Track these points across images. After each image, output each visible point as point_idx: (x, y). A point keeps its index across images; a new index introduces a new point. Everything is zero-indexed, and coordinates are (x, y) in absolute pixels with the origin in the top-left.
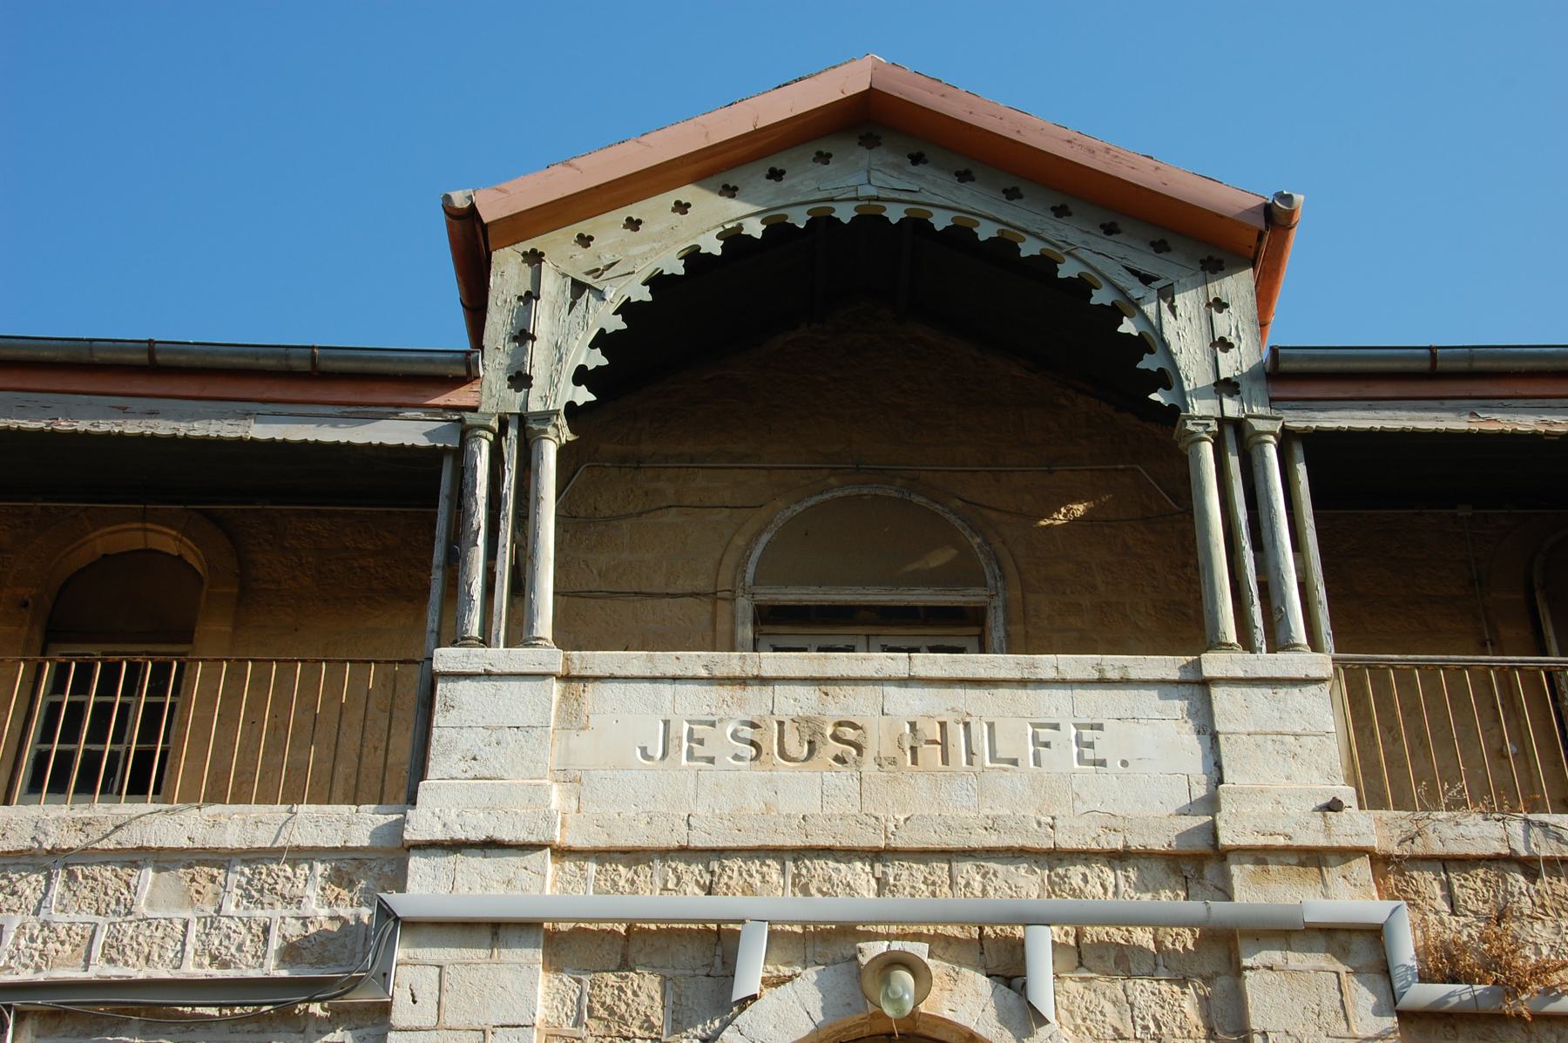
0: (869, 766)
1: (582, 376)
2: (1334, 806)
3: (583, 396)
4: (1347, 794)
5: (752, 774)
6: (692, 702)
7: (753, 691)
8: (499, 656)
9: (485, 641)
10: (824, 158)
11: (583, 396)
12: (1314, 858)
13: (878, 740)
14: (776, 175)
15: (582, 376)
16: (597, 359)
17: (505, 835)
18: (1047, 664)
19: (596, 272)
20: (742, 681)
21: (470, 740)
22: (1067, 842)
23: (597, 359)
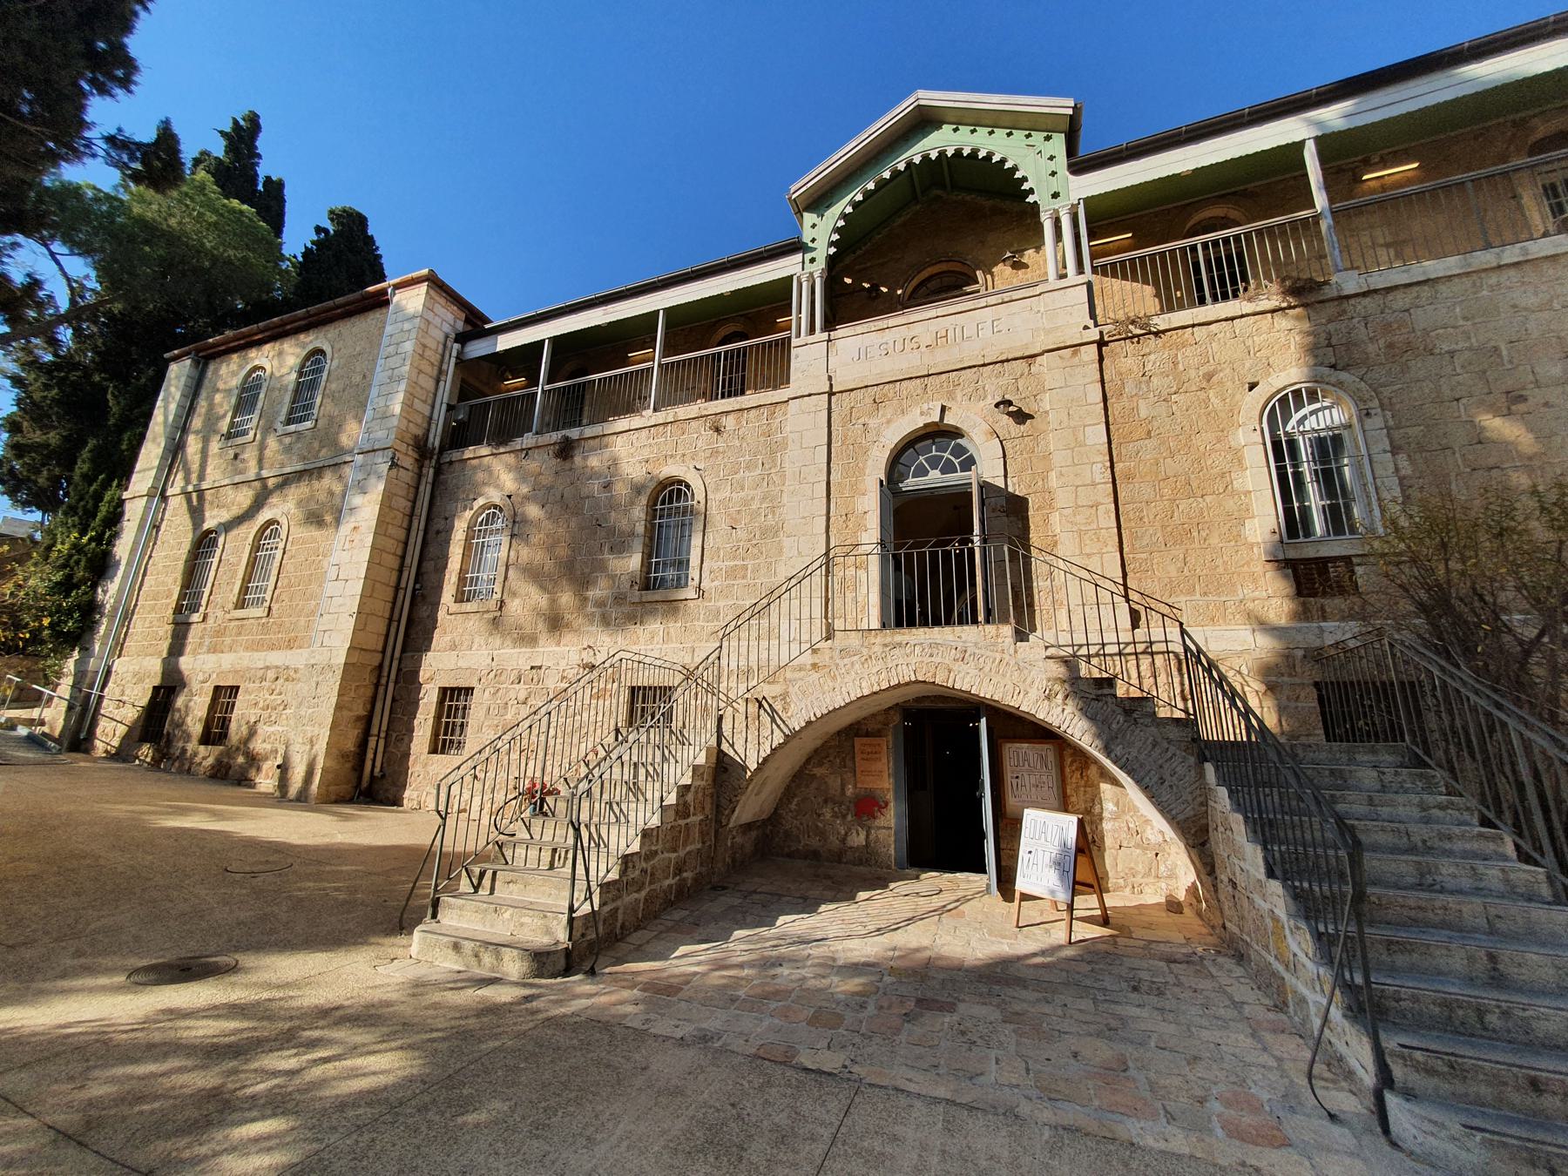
0: (923, 349)
2: (1086, 328)
3: (832, 250)
15: (831, 244)
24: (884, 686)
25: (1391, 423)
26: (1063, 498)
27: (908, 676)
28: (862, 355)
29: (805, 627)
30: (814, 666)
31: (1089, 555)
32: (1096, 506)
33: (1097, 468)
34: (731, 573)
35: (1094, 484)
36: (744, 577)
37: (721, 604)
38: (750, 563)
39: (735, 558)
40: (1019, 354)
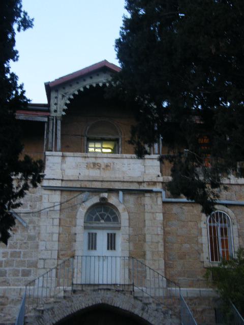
1: (64, 110)
2: (159, 176)
3: (64, 113)
4: (160, 174)
5: (87, 171)
6: (79, 160)
7: (87, 159)
8: (54, 153)
9: (52, 151)
10: (98, 75)
11: (64, 113)
12: (155, 183)
13: (103, 166)
14: (91, 78)
15: (64, 110)
16: (66, 108)
17: (55, 178)
18: (125, 155)
19: (66, 94)
20: (85, 157)
21: (51, 165)
22: (125, 180)
23: (66, 108)
24: (90, 305)
25: (239, 228)
26: (148, 237)
27: (99, 301)
28: (77, 166)
29: (45, 282)
30: (65, 297)
31: (155, 260)
32: (158, 242)
33: (159, 229)
34: (13, 254)
35: (158, 235)
36: (19, 257)
37: (7, 269)
38: (22, 251)
39: (15, 248)
40: (136, 180)
